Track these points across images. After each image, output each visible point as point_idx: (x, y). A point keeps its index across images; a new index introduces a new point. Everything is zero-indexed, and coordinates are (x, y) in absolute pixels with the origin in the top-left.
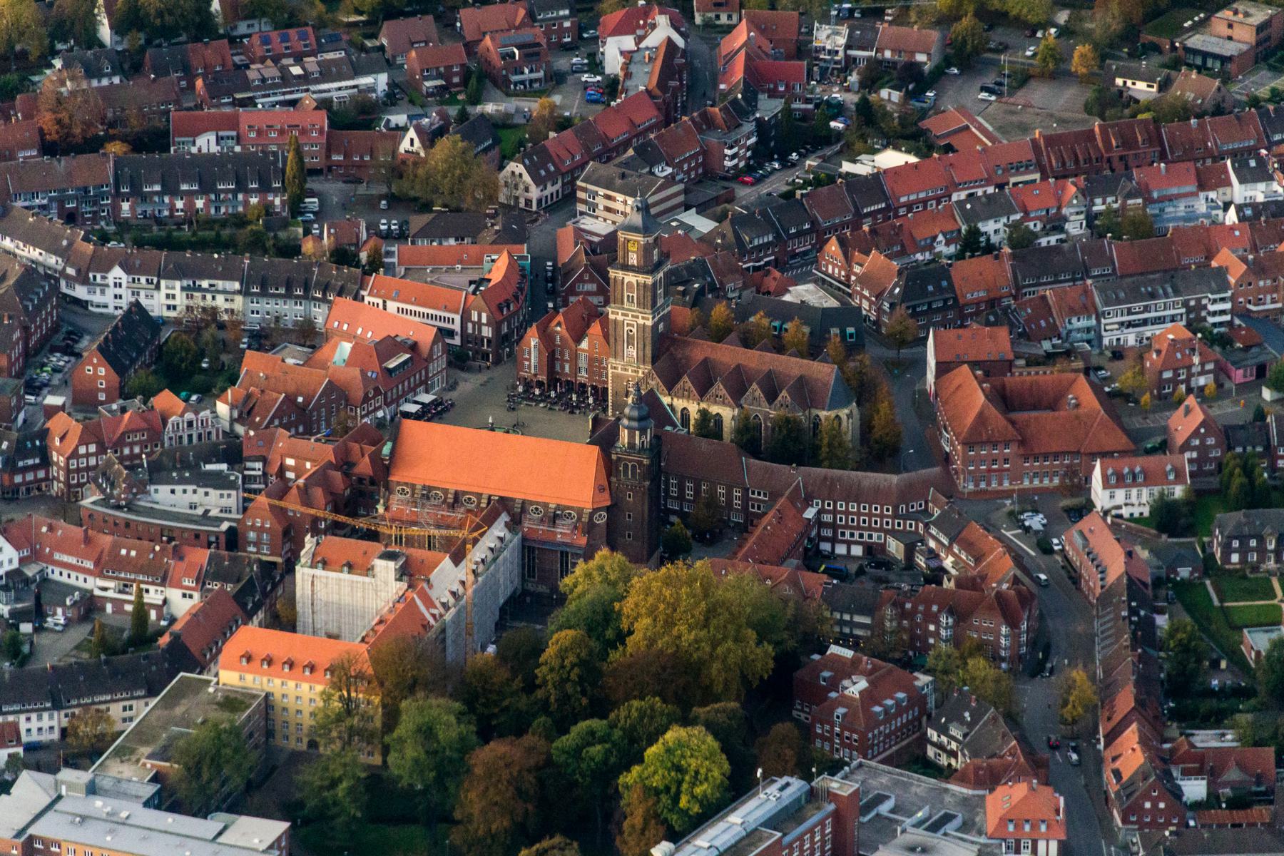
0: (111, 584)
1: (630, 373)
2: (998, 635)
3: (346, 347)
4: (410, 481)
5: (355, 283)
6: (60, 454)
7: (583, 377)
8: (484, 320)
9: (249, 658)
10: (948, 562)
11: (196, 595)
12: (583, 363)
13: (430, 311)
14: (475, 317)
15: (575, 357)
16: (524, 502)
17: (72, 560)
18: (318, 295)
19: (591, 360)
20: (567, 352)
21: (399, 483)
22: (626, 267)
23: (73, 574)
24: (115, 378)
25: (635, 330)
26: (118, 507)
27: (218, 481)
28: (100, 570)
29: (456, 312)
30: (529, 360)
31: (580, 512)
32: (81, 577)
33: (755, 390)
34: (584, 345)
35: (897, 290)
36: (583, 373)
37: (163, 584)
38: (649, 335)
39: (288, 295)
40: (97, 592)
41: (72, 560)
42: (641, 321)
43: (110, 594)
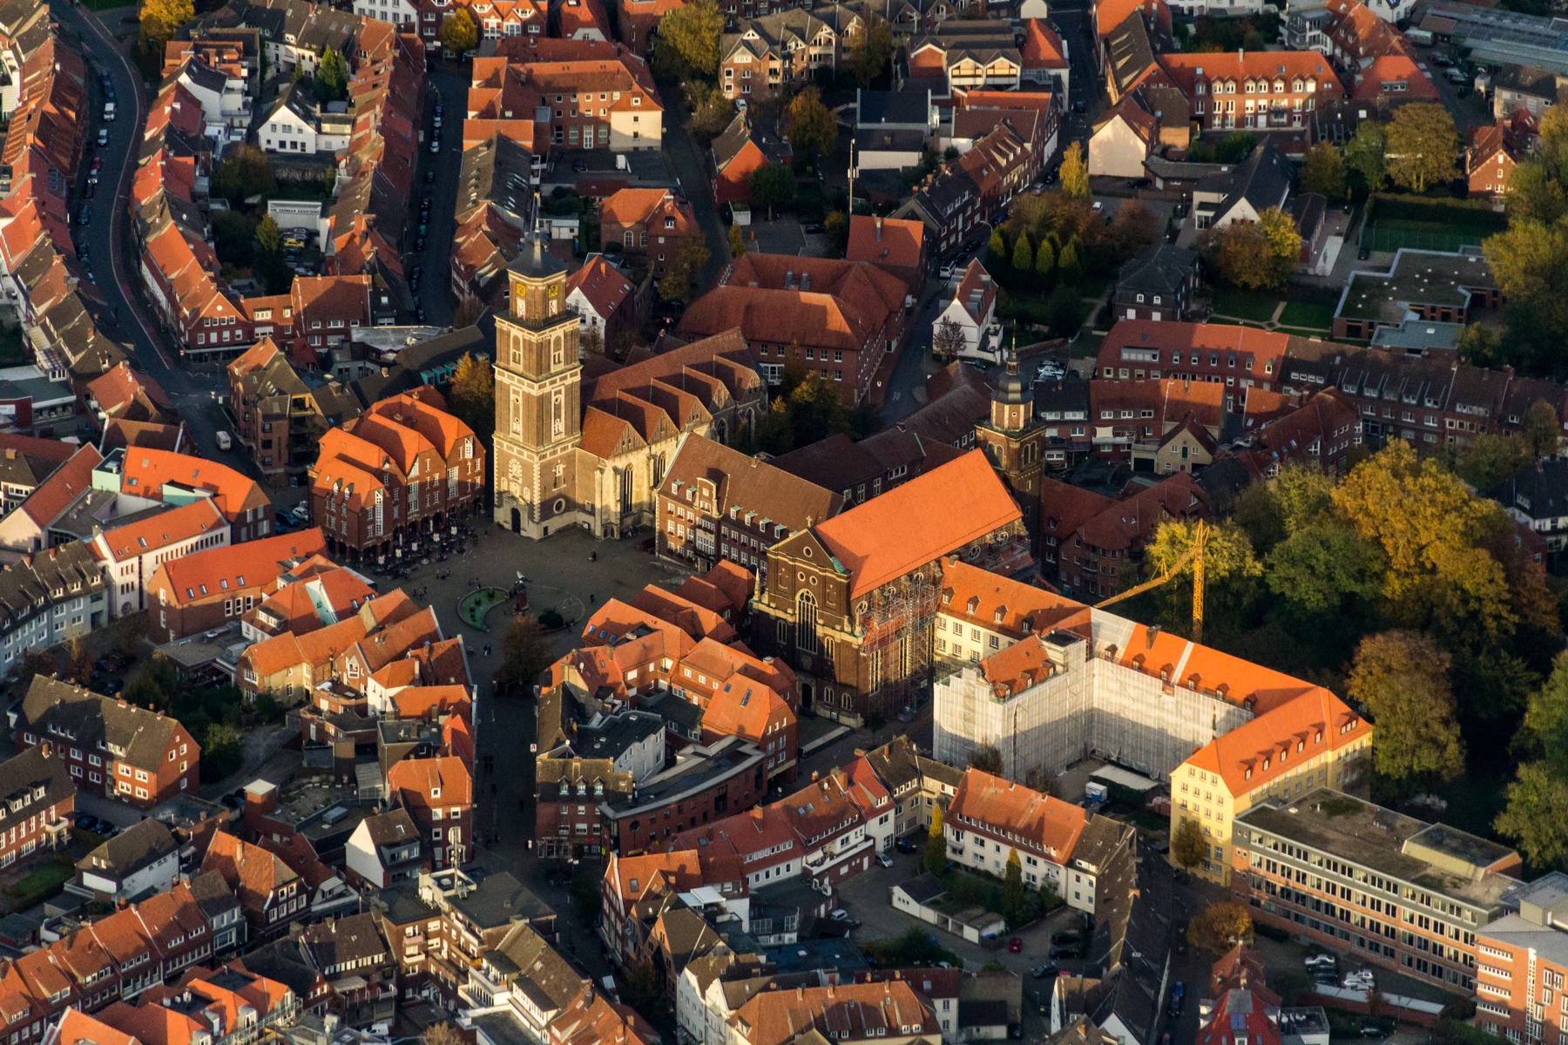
0: (818, 855)
1: (559, 453)
2: (1351, 436)
3: (315, 587)
4: (864, 592)
5: (85, 558)
6: (445, 803)
7: (414, 514)
8: (261, 516)
9: (1250, 765)
10: (1104, 434)
11: (891, 814)
12: (413, 497)
13: (194, 540)
14: (249, 519)
15: (408, 489)
16: (967, 546)
17: (766, 853)
18: (60, 594)
19: (422, 486)
20: (396, 491)
21: (858, 599)
22: (550, 322)
23: (772, 870)
24: (197, 748)
25: (562, 397)
26: (636, 803)
27: (621, 735)
28: (804, 848)
29: (218, 524)
30: (373, 522)
31: (1009, 526)
32: (783, 867)
33: (721, 393)
34: (415, 472)
35: (385, 300)
36: (413, 510)
37: (862, 821)
38: (577, 394)
39: (36, 613)
40: (816, 870)
41: (766, 853)
42: (569, 381)
43: (828, 864)
